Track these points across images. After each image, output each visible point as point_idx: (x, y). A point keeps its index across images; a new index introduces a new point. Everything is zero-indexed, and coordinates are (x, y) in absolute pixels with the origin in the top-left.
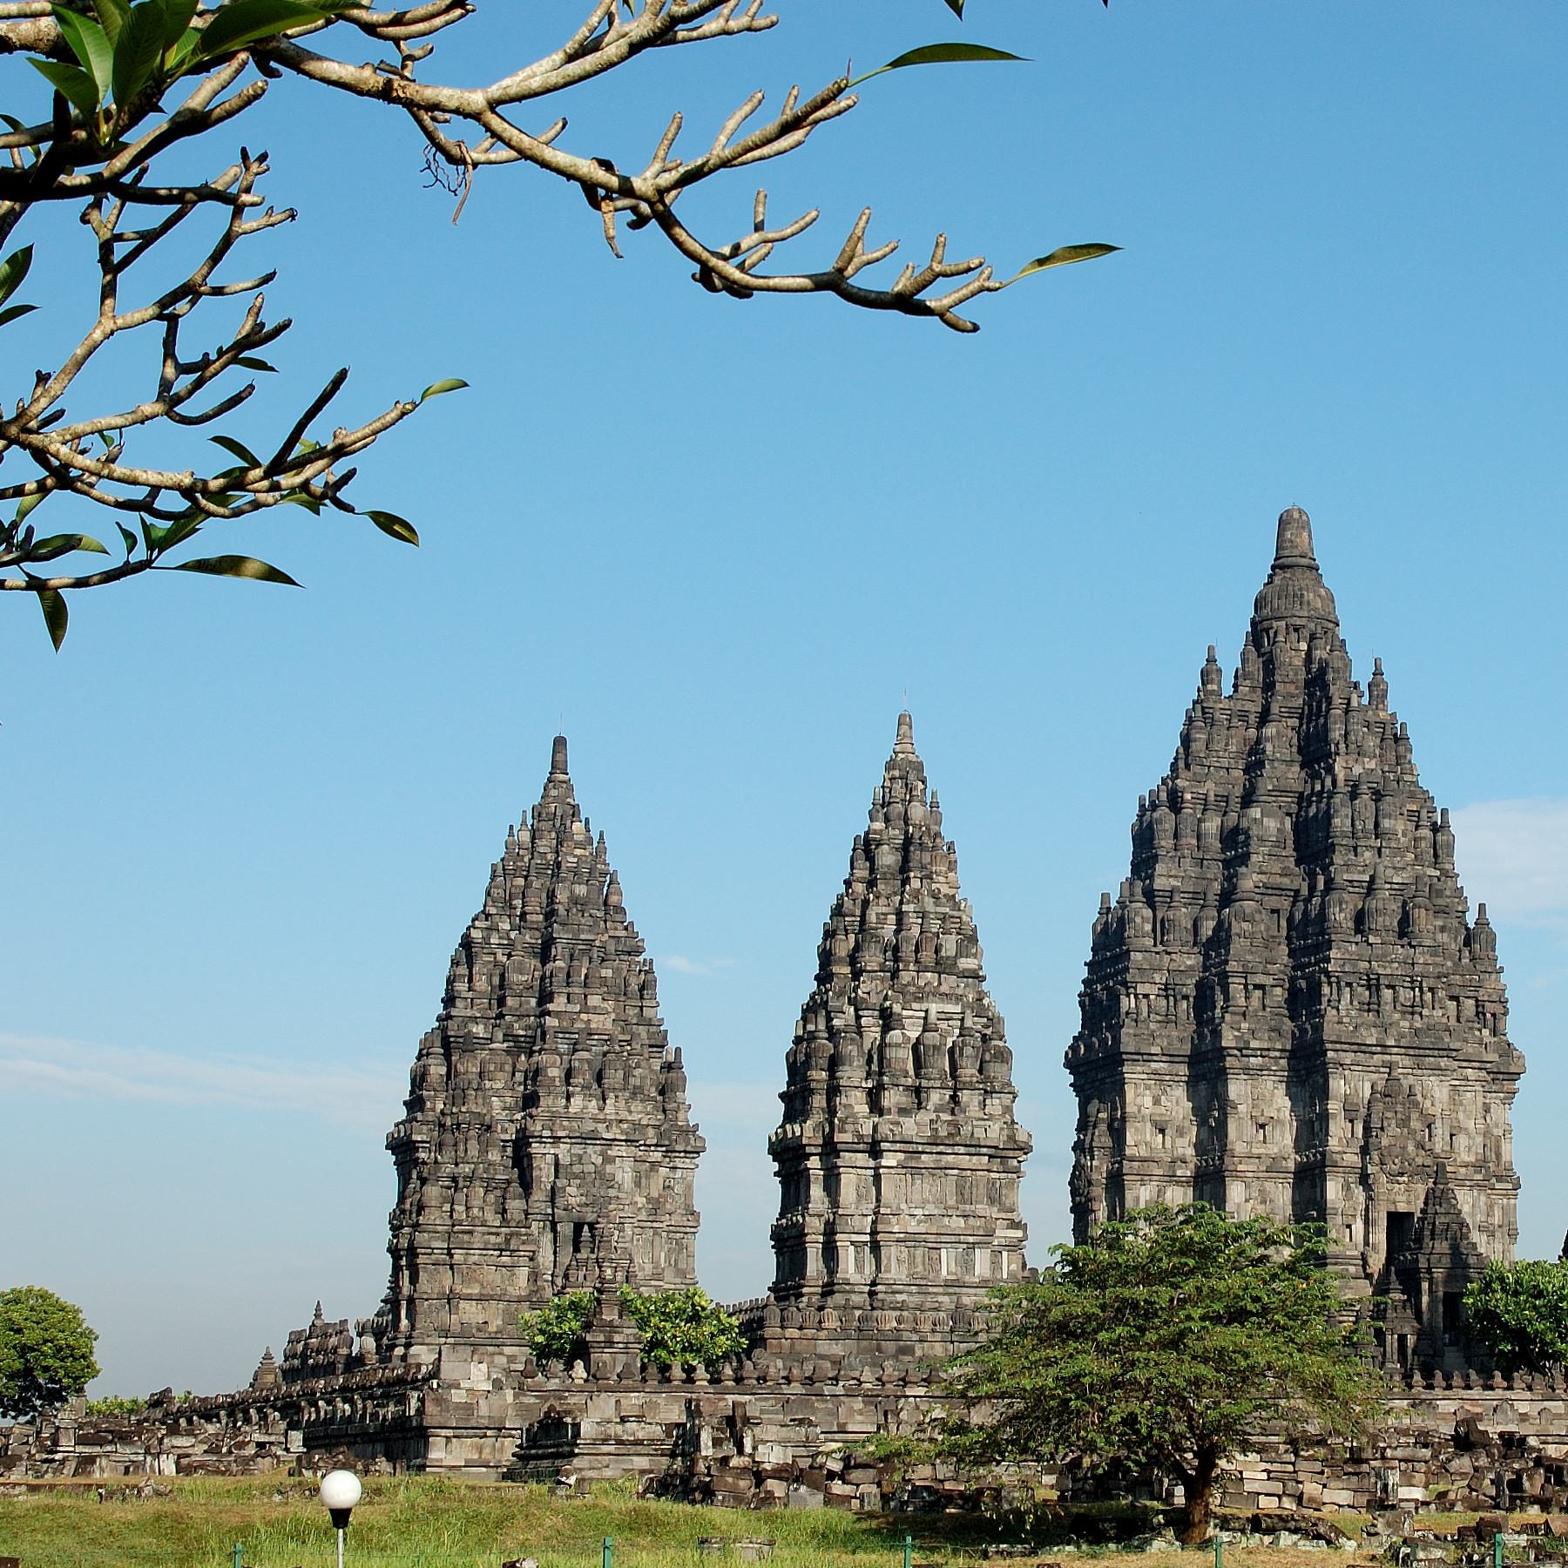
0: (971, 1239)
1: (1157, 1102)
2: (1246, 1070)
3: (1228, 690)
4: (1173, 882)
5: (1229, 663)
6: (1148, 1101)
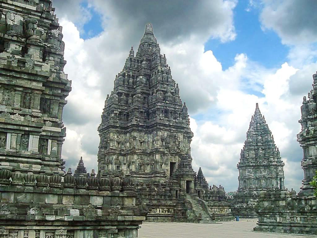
0: (27, 129)
1: (118, 137)
2: (138, 130)
3: (135, 56)
4: (123, 91)
5: (136, 51)
6: (116, 137)
